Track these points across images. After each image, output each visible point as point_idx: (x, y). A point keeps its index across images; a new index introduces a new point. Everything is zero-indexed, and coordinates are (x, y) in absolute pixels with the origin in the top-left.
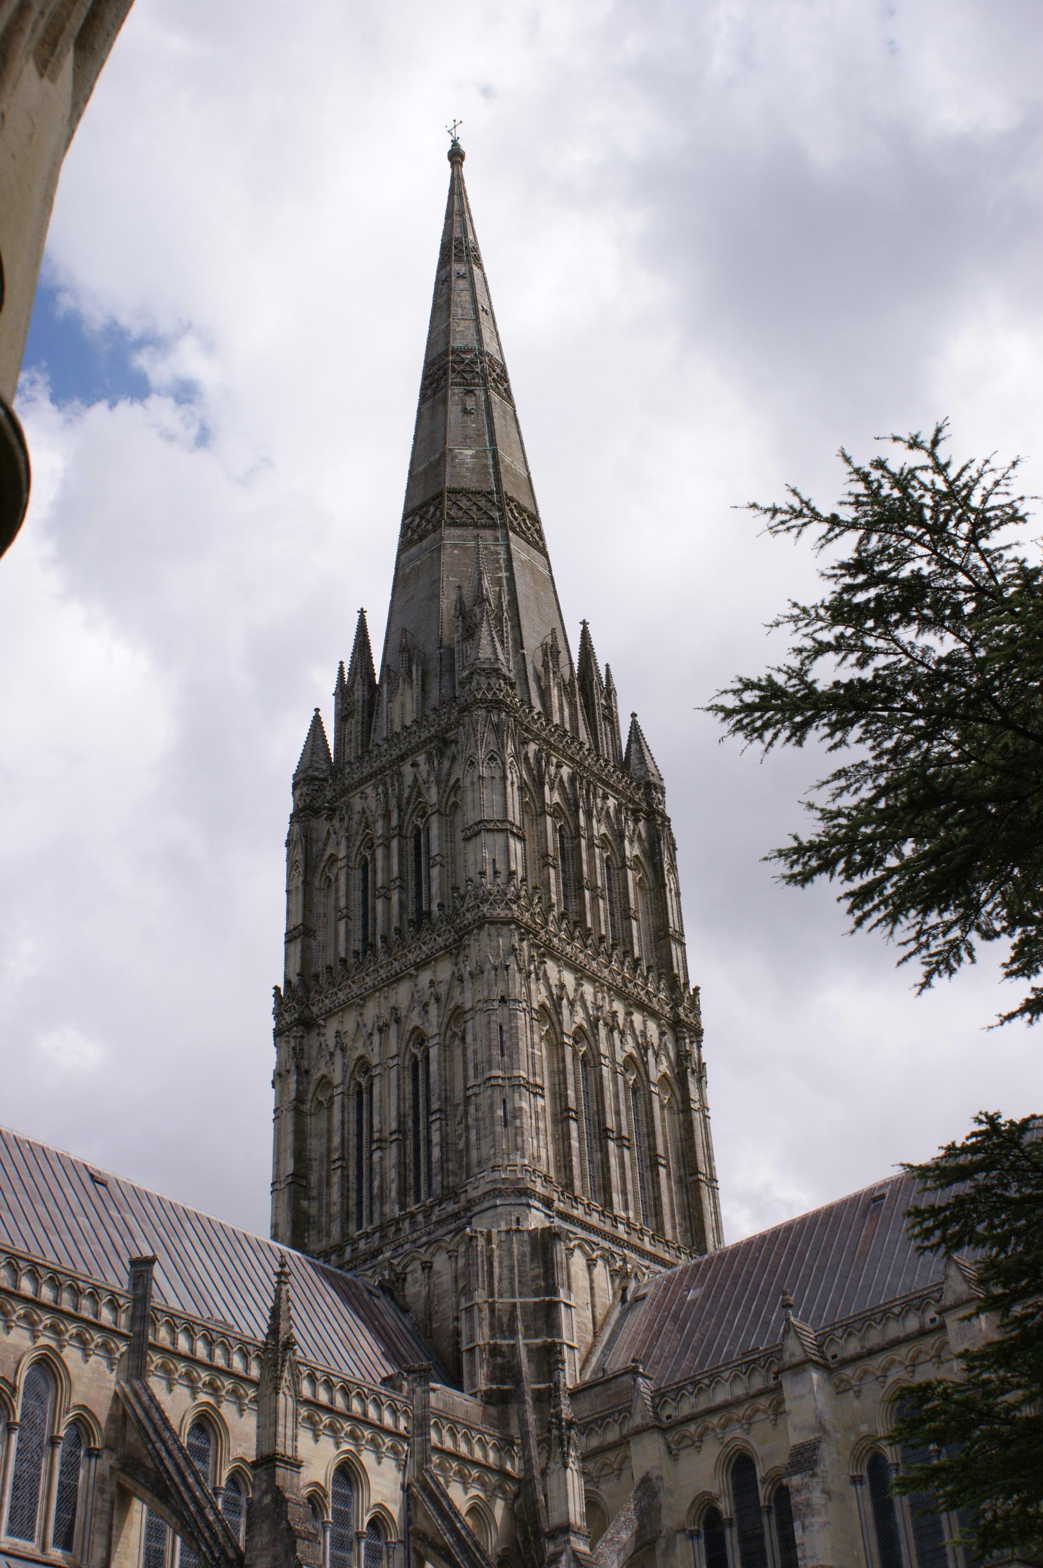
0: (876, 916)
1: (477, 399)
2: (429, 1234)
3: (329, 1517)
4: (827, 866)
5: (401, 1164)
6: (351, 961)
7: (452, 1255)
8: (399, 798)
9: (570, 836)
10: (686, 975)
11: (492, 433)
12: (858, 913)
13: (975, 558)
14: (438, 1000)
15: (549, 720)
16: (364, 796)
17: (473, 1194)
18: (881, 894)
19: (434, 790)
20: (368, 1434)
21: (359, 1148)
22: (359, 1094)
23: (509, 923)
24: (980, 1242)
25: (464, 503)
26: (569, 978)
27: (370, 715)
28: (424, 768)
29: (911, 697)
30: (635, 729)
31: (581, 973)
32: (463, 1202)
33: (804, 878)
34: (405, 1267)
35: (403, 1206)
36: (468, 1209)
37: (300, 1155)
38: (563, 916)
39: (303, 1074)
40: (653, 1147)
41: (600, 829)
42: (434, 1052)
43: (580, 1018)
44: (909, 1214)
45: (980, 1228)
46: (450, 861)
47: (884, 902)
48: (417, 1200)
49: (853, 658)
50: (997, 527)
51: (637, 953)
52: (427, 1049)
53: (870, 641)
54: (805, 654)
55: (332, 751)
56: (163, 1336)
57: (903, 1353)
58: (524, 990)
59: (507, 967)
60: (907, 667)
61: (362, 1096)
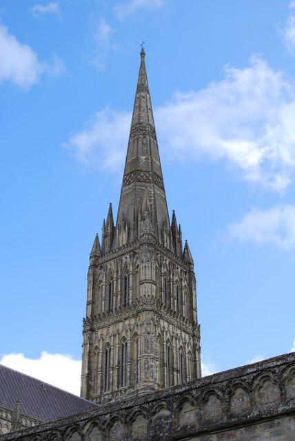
5: (118, 375)
8: (121, 267)
9: (167, 282)
11: (151, 151)
25: (142, 174)
26: (166, 324)
28: (128, 259)
31: (169, 323)
32: (135, 390)
37: (89, 368)
38: (165, 307)
39: (91, 344)
40: (186, 372)
41: (176, 278)
42: (129, 345)
46: (134, 288)
61: (107, 353)
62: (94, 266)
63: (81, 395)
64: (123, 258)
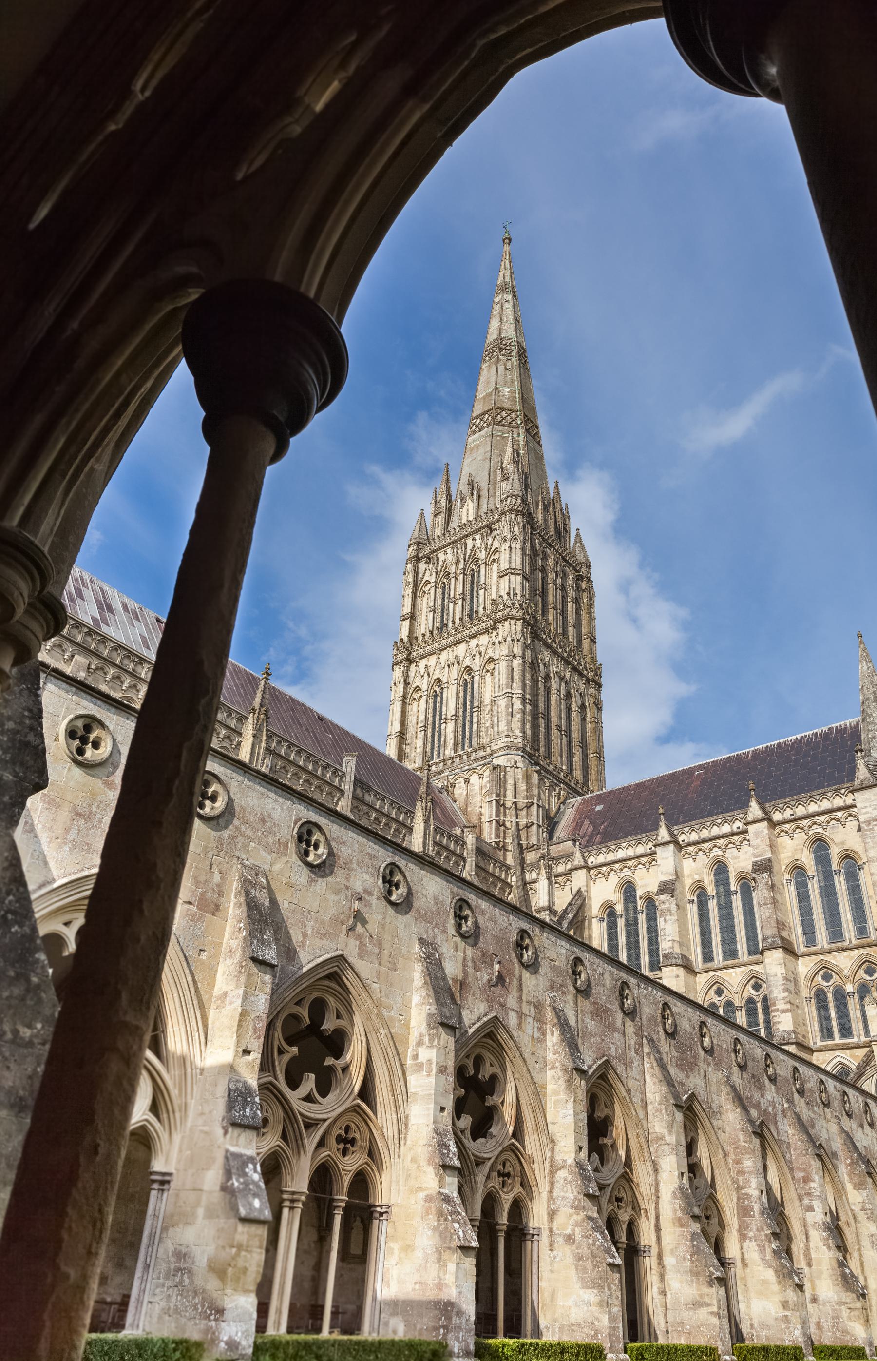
1: (512, 363)
5: (456, 731)
6: (435, 632)
7: (481, 777)
14: (480, 654)
16: (446, 553)
17: (494, 748)
19: (484, 552)
21: (434, 722)
22: (435, 696)
27: (450, 516)
28: (478, 541)
30: (578, 535)
34: (456, 780)
35: (455, 751)
42: (476, 679)
48: (463, 749)
52: (473, 677)
57: (721, 842)
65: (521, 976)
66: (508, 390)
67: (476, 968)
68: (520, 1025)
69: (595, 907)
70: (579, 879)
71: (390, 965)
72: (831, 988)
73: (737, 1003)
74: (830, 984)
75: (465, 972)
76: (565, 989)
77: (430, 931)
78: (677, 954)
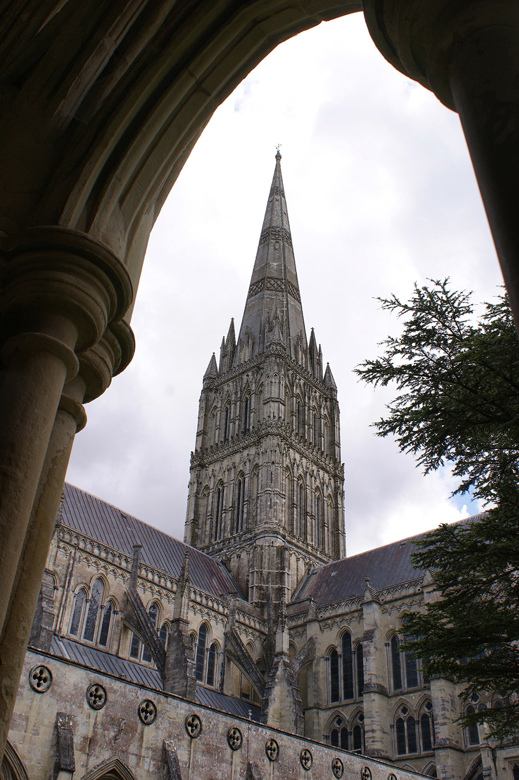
0: (409, 448)
1: (280, 245)
2: (240, 545)
3: (197, 642)
4: (392, 429)
5: (232, 519)
6: (220, 444)
7: (248, 553)
8: (241, 387)
10: (340, 459)
11: (284, 258)
12: (402, 446)
13: (454, 324)
14: (250, 461)
15: (297, 363)
17: (257, 532)
18: (411, 440)
19: (254, 385)
20: (213, 613)
21: (218, 512)
22: (219, 492)
23: (278, 435)
24: (437, 566)
25: (272, 282)
26: (297, 456)
27: (233, 356)
29: (427, 371)
30: (328, 368)
31: (302, 455)
32: (253, 534)
33: (385, 434)
34: (231, 556)
35: (232, 534)
36: (255, 537)
37: (196, 513)
38: (297, 434)
39: (199, 484)
40: (323, 520)
42: (247, 480)
43: (300, 471)
44: (412, 555)
45: (437, 561)
46: (258, 411)
47: (412, 443)
49: (407, 356)
50: (462, 314)
51: (323, 450)
52: (245, 478)
53: (414, 351)
54: (390, 353)
55: (218, 369)
56: (143, 572)
57: (407, 601)
58: (281, 460)
59: (276, 451)
60: (426, 361)
61: (220, 493)
62: (206, 390)
63: (185, 541)
64: (245, 377)
65: (142, 732)
66: (276, 264)
67: (105, 729)
68: (138, 764)
69: (321, 650)
70: (313, 630)
71: (33, 732)
72: (478, 706)
73: (416, 719)
74: (477, 702)
75: (94, 732)
76: (180, 737)
77: (69, 708)
78: (374, 684)
